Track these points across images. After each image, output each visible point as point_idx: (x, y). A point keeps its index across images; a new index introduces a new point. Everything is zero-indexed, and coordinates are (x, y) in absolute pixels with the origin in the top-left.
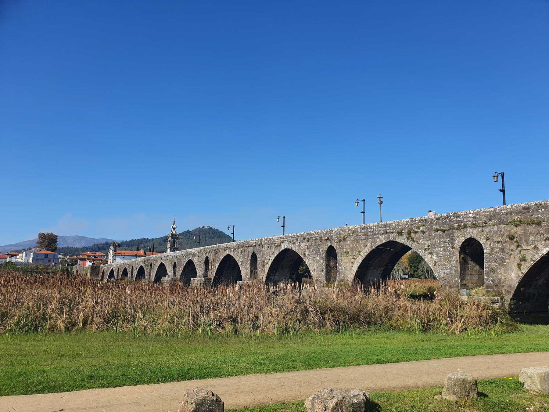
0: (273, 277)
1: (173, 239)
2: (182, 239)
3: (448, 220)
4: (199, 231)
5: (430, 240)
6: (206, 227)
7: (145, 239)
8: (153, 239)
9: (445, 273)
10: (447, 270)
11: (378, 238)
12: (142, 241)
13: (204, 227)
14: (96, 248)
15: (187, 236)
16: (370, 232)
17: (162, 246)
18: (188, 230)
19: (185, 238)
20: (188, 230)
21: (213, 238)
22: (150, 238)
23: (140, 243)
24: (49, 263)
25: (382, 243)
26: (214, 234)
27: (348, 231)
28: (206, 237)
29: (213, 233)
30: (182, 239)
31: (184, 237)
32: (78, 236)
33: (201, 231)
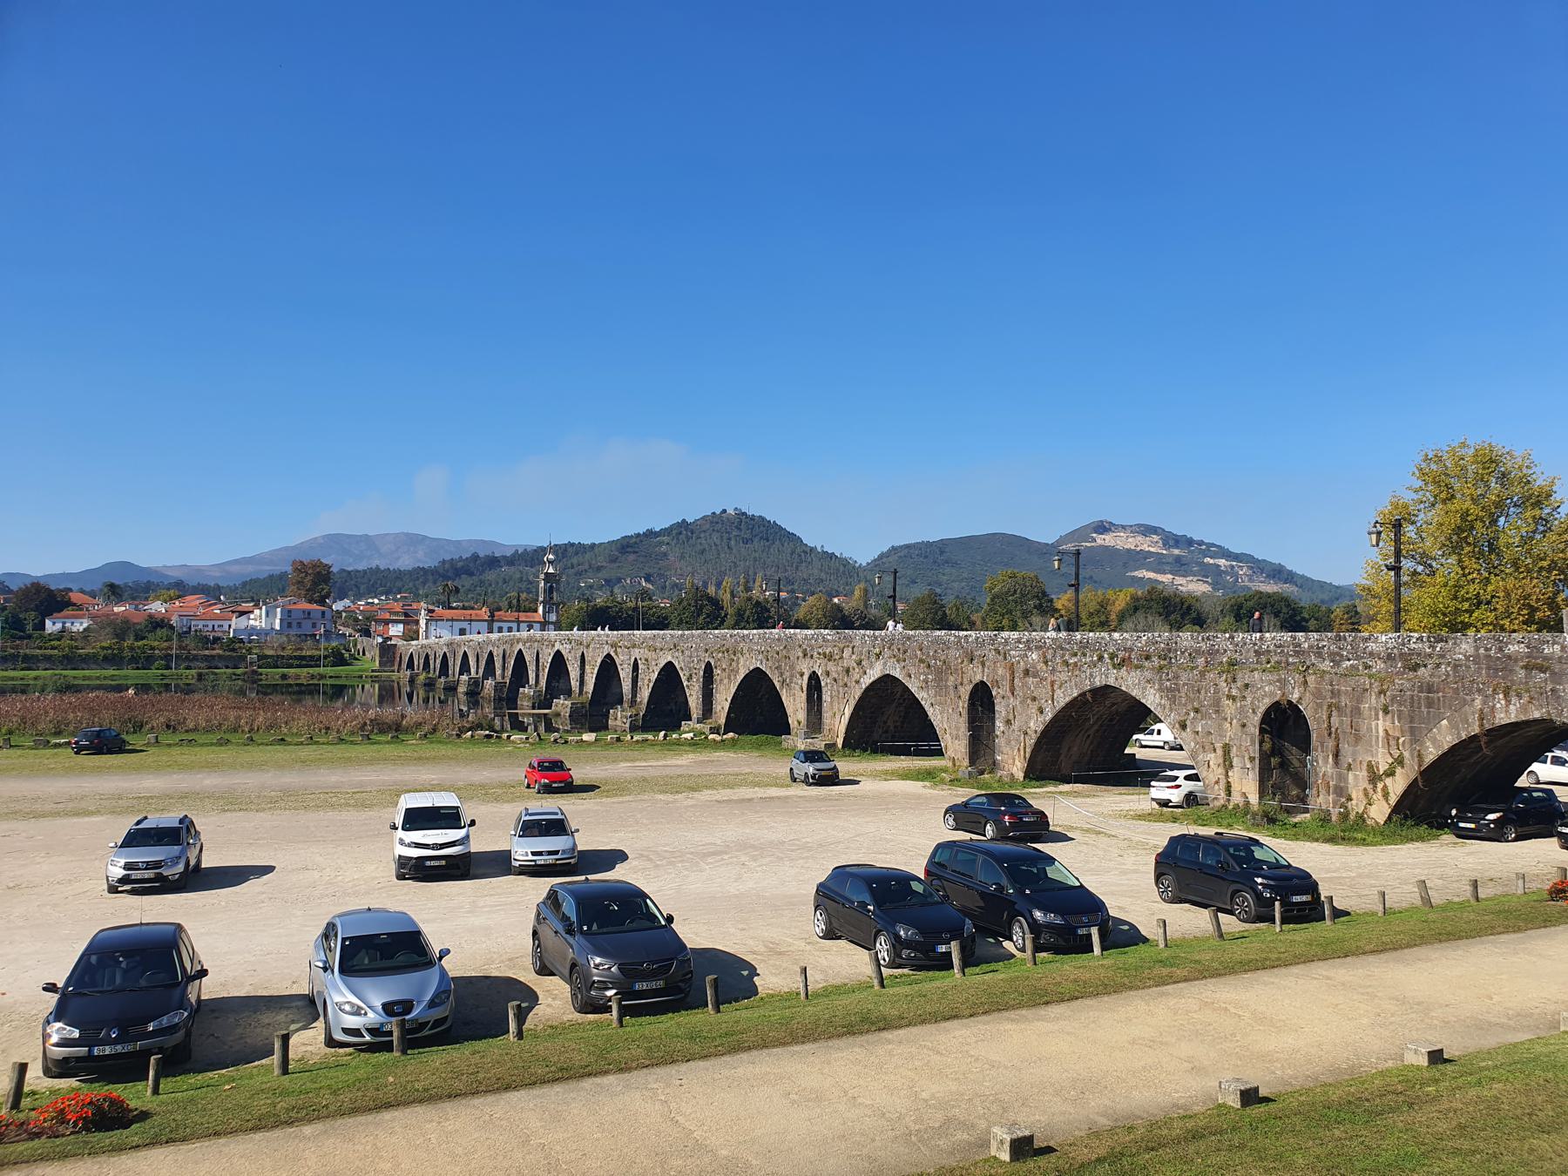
1: (549, 585)
2: (668, 544)
4: (712, 522)
6: (731, 511)
7: (572, 545)
8: (593, 545)
12: (566, 550)
13: (724, 511)
14: (448, 571)
15: (681, 536)
17: (617, 564)
18: (684, 520)
19: (675, 541)
20: (684, 520)
21: (750, 541)
22: (587, 542)
23: (560, 555)
24: (314, 629)
26: (752, 529)
28: (730, 539)
29: (750, 527)
30: (668, 544)
31: (673, 540)
32: (407, 535)
33: (717, 523)
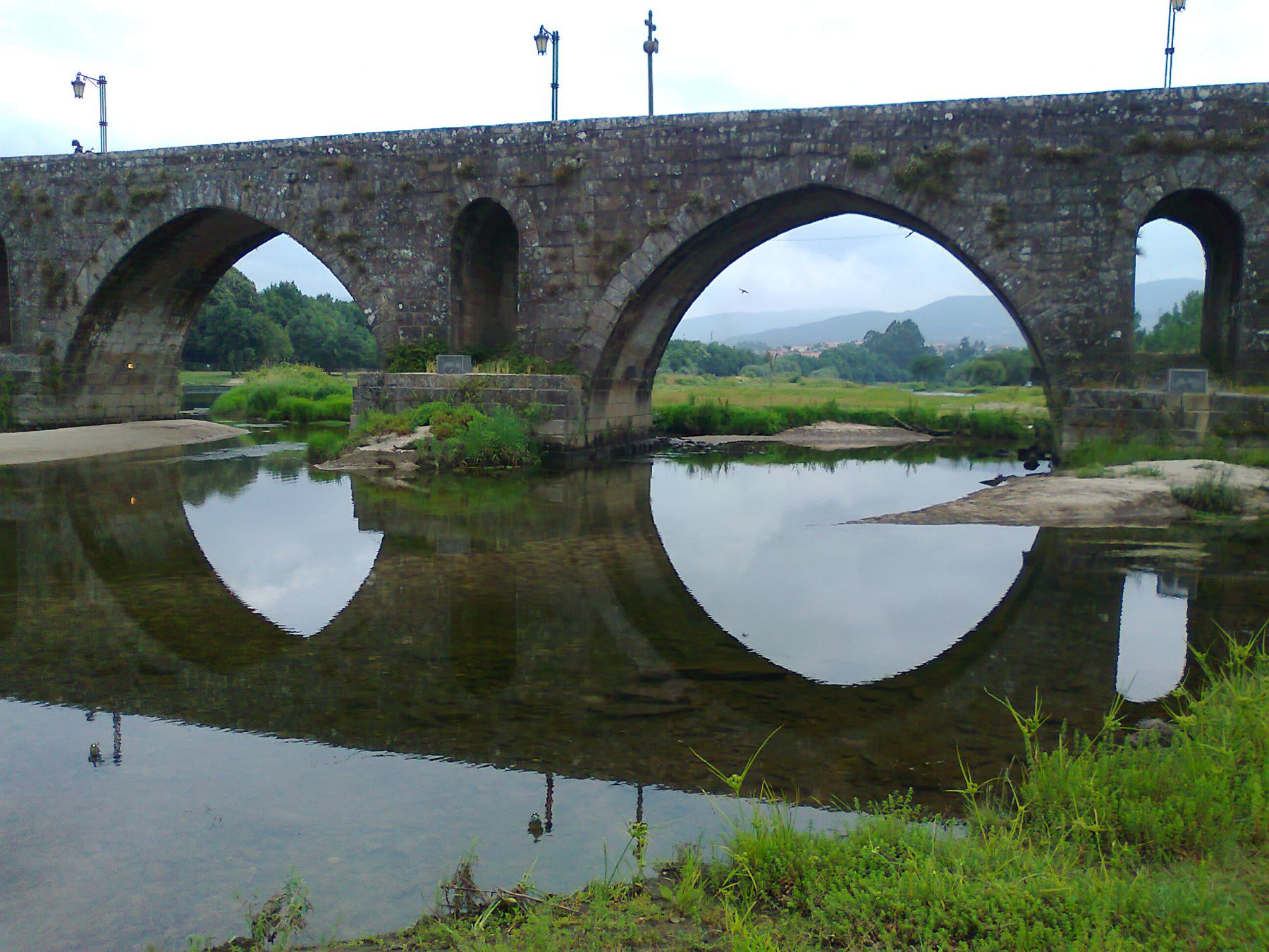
0: (103, 336)
3: (1094, 119)
5: (1006, 190)
9: (1067, 314)
10: (1077, 302)
11: (749, 172)
16: (711, 147)
25: (769, 193)
27: (589, 139)
